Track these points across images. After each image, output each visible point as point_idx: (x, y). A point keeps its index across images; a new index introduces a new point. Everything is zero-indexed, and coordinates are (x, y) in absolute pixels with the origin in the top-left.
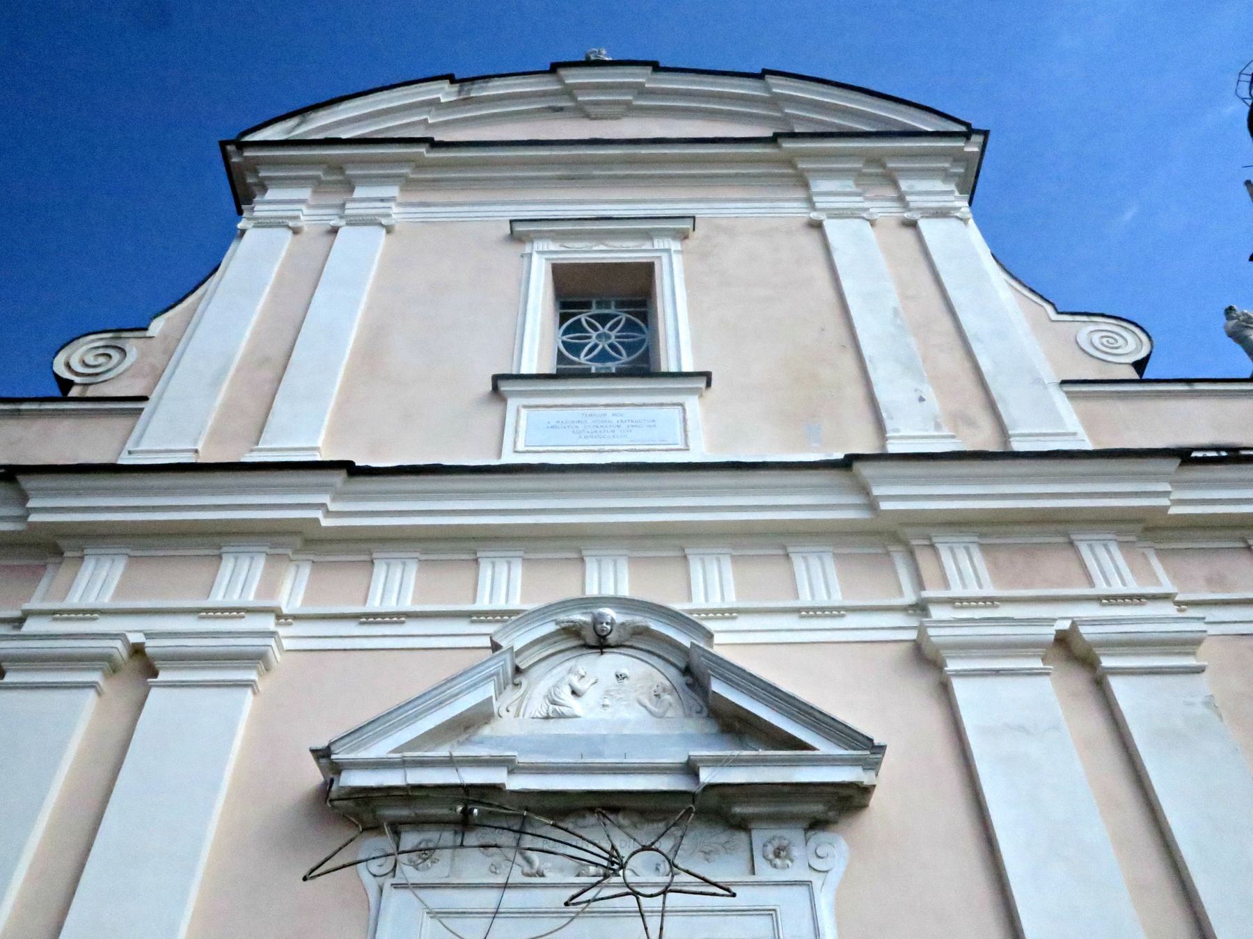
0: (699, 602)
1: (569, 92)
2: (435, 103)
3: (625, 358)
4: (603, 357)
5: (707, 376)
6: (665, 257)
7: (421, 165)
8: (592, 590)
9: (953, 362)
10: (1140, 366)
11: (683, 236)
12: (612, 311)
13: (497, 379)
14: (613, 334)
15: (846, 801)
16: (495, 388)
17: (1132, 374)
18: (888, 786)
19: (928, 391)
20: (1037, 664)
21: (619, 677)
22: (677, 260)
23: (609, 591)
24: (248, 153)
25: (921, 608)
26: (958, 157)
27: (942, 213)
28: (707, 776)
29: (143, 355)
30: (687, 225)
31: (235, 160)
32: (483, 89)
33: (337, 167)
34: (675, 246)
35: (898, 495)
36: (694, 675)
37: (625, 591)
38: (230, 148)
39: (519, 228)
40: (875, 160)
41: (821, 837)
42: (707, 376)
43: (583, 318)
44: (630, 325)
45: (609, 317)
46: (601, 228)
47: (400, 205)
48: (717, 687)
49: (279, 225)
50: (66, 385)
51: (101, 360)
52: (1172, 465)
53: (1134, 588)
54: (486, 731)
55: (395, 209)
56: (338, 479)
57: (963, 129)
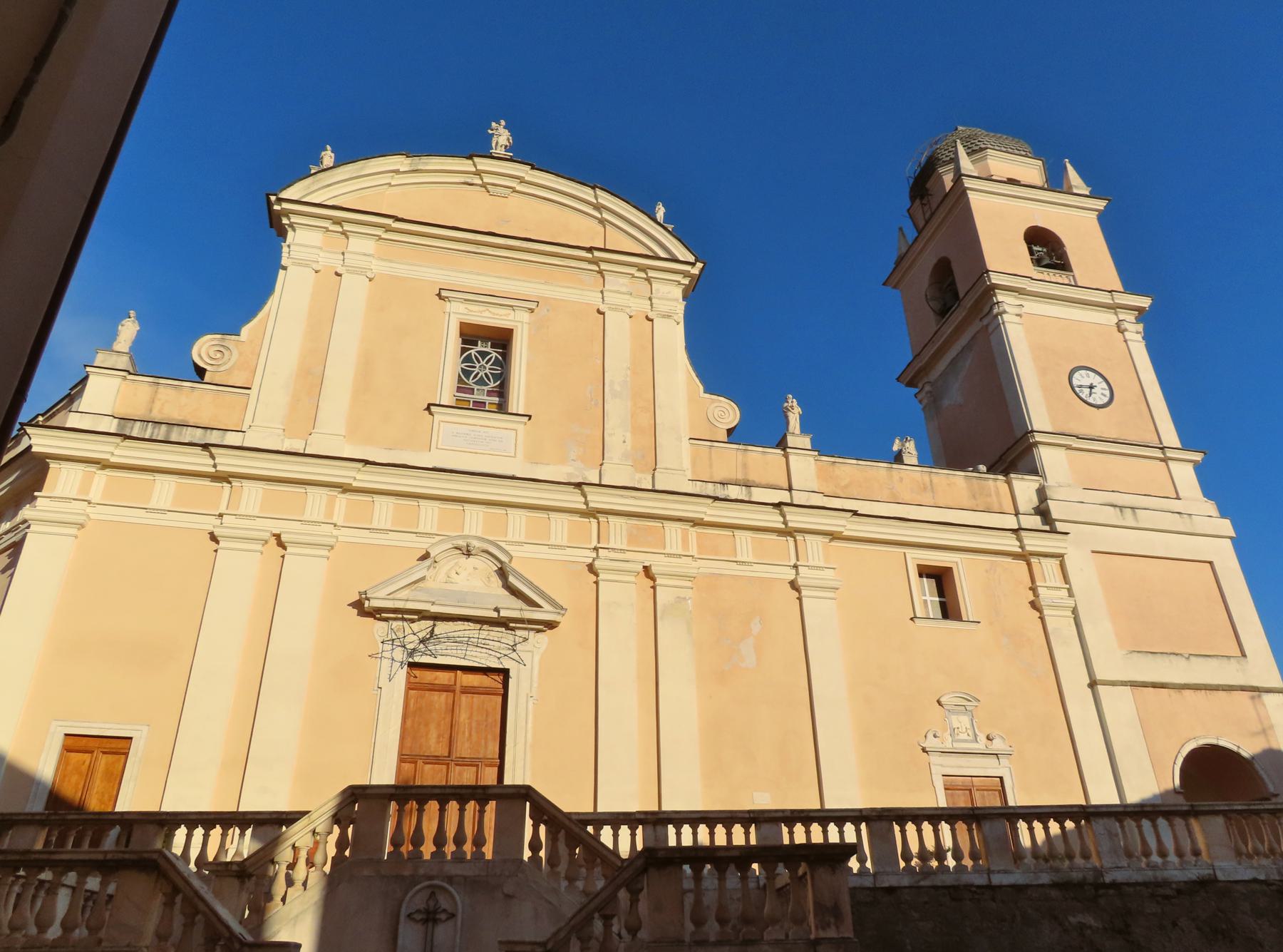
0: (510, 538)
1: (478, 173)
2: (397, 172)
3: (492, 385)
4: (481, 382)
5: (530, 417)
6: (519, 325)
7: (388, 229)
8: (466, 532)
9: (646, 420)
10: (730, 431)
11: (532, 311)
12: (488, 349)
13: (429, 405)
14: (488, 366)
15: (551, 625)
16: (428, 408)
17: (724, 437)
18: (565, 622)
19: (628, 435)
20: (632, 579)
21: (475, 568)
22: (526, 327)
23: (473, 533)
24: (285, 205)
25: (596, 549)
26: (685, 274)
27: (667, 316)
28: (503, 613)
29: (240, 354)
30: (533, 305)
31: (276, 207)
32: (426, 164)
33: (338, 222)
34: (525, 316)
35: (598, 499)
36: (502, 573)
37: (479, 534)
38: (273, 198)
39: (444, 293)
40: (643, 269)
41: (540, 635)
42: (530, 417)
43: (473, 352)
44: (497, 362)
45: (488, 349)
46: (490, 298)
47: (380, 259)
48: (511, 579)
49: (307, 266)
50: (201, 372)
51: (219, 355)
52: (710, 501)
53: (680, 551)
54: (421, 585)
55: (374, 262)
56: (360, 465)
57: (692, 259)
